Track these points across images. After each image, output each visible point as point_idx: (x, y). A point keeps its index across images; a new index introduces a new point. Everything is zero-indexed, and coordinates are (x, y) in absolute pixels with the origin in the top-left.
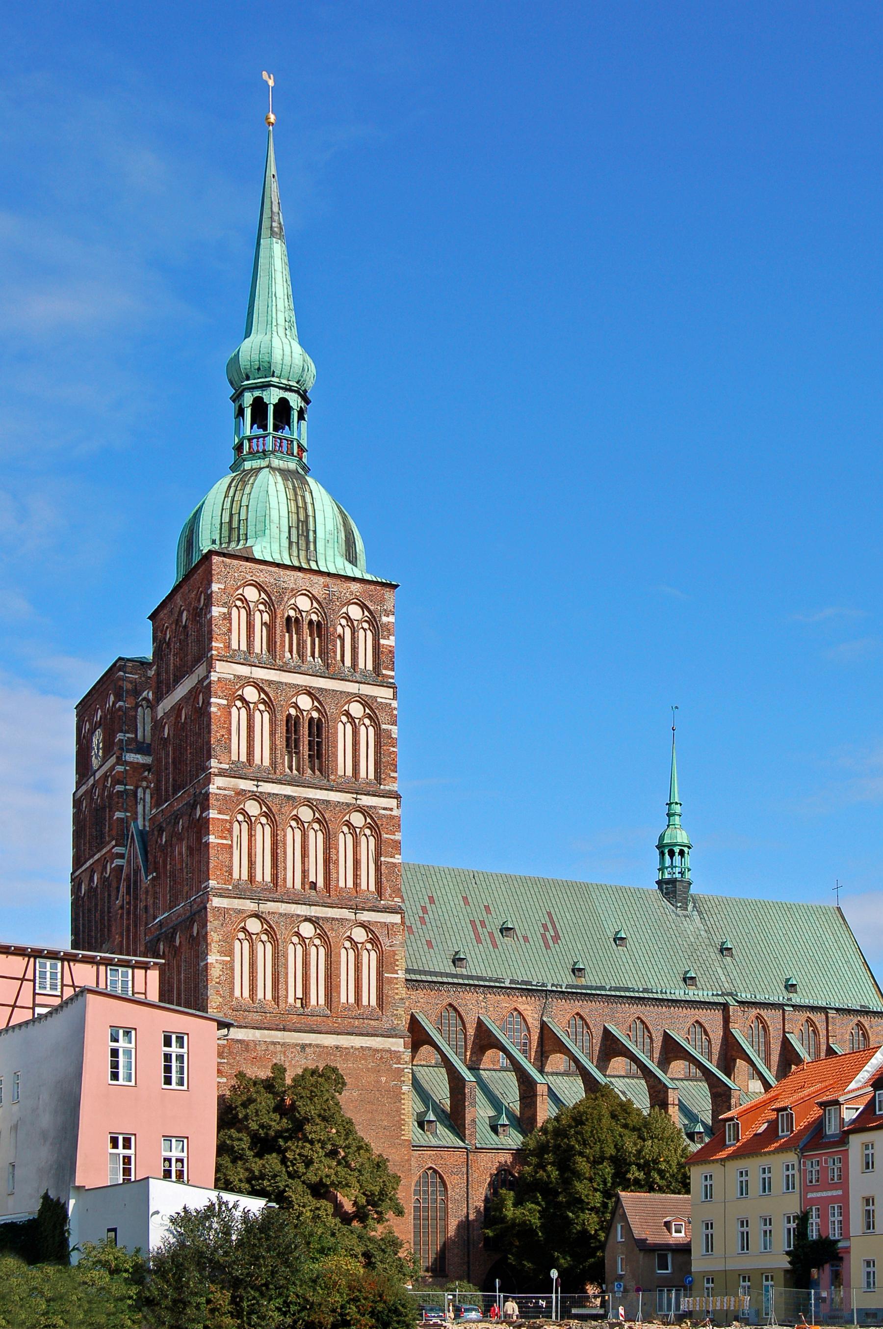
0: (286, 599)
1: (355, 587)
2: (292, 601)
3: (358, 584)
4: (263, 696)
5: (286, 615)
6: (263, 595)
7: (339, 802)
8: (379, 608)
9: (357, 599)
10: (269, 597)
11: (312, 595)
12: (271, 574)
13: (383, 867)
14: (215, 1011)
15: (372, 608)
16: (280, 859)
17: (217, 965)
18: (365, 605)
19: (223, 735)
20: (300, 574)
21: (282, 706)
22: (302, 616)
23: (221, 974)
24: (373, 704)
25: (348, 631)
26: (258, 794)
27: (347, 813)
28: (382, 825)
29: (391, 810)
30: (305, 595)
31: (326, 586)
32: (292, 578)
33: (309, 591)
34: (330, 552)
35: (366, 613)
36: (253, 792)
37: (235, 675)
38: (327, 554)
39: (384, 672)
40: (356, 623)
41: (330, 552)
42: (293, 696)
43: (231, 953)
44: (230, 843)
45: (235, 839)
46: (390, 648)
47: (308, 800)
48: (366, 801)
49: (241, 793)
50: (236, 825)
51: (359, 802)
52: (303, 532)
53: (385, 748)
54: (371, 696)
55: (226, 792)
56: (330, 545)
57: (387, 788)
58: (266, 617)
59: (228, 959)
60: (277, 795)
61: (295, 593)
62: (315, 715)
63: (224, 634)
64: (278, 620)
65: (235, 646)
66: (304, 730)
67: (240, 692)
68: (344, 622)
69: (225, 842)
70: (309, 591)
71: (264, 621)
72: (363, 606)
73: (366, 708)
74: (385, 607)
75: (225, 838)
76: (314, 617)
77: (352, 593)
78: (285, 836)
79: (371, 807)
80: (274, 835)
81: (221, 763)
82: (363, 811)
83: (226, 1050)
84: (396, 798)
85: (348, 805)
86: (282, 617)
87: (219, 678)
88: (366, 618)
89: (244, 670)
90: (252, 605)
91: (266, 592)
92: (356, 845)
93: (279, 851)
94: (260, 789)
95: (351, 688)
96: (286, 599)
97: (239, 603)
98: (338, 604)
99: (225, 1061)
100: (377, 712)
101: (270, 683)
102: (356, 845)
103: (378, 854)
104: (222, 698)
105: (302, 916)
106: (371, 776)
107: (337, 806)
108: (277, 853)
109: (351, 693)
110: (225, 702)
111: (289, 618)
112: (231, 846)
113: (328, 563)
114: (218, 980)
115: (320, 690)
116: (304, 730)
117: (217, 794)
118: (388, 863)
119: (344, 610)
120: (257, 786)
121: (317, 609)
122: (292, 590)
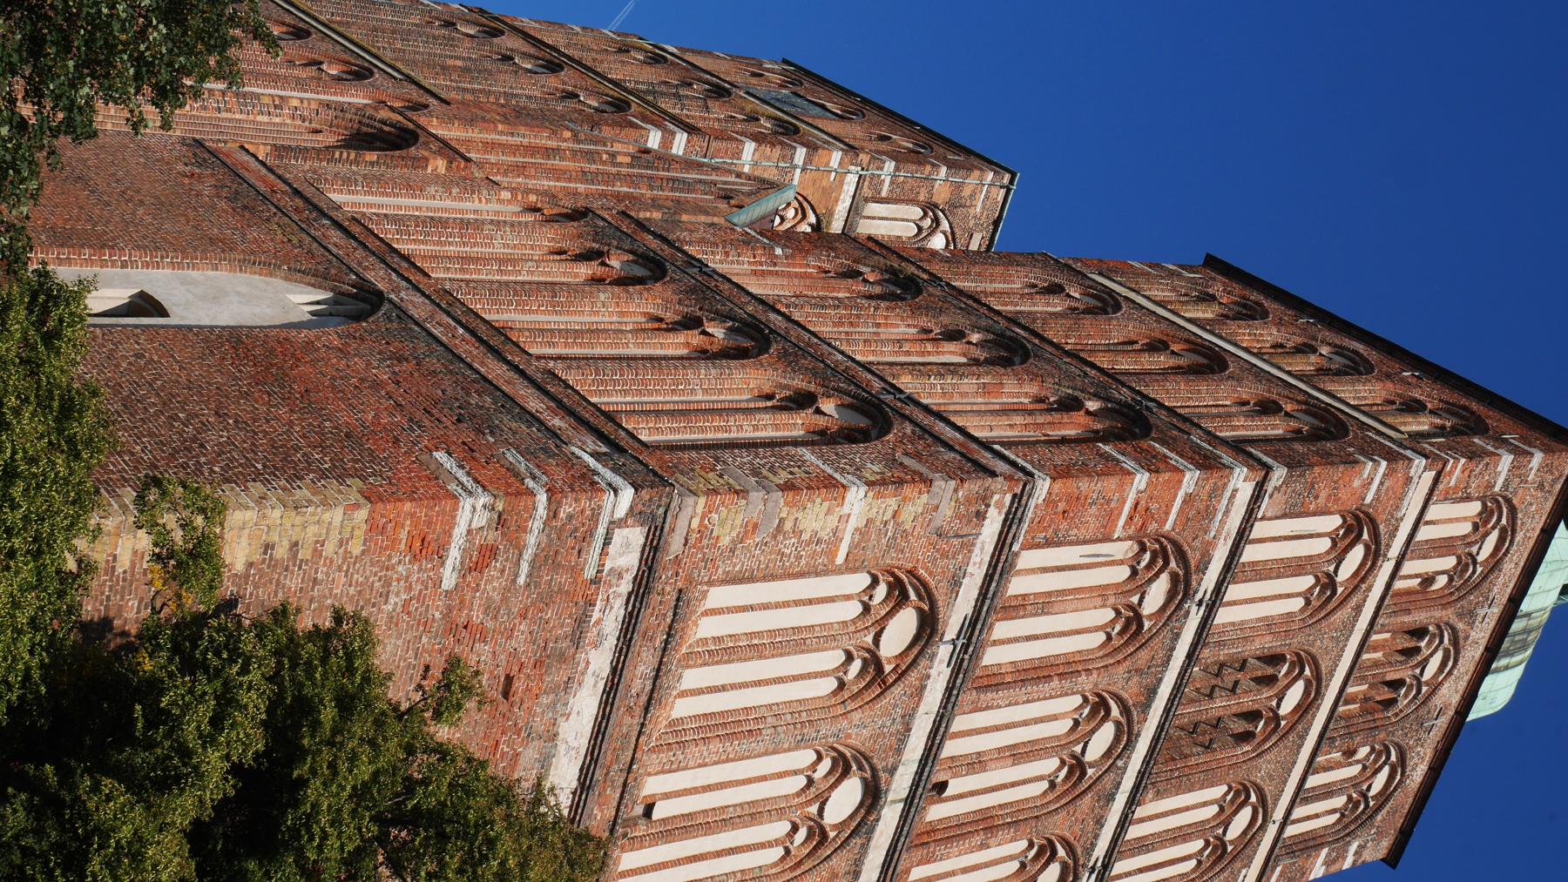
11: (1441, 683)
14: (695, 523)
15: (1379, 818)
17: (832, 521)
18: (1387, 800)
19: (1316, 497)
23: (805, 537)
33: (1450, 673)
36: (1196, 592)
37: (1402, 519)
43: (850, 567)
59: (840, 559)
70: (1450, 673)
72: (1385, 795)
83: (563, 578)
87: (1412, 478)
91: (1485, 577)
99: (521, 580)
105: (889, 784)
109: (1276, 806)
110: (1368, 500)
112: (1107, 539)
114: (788, 526)
117: (1225, 485)
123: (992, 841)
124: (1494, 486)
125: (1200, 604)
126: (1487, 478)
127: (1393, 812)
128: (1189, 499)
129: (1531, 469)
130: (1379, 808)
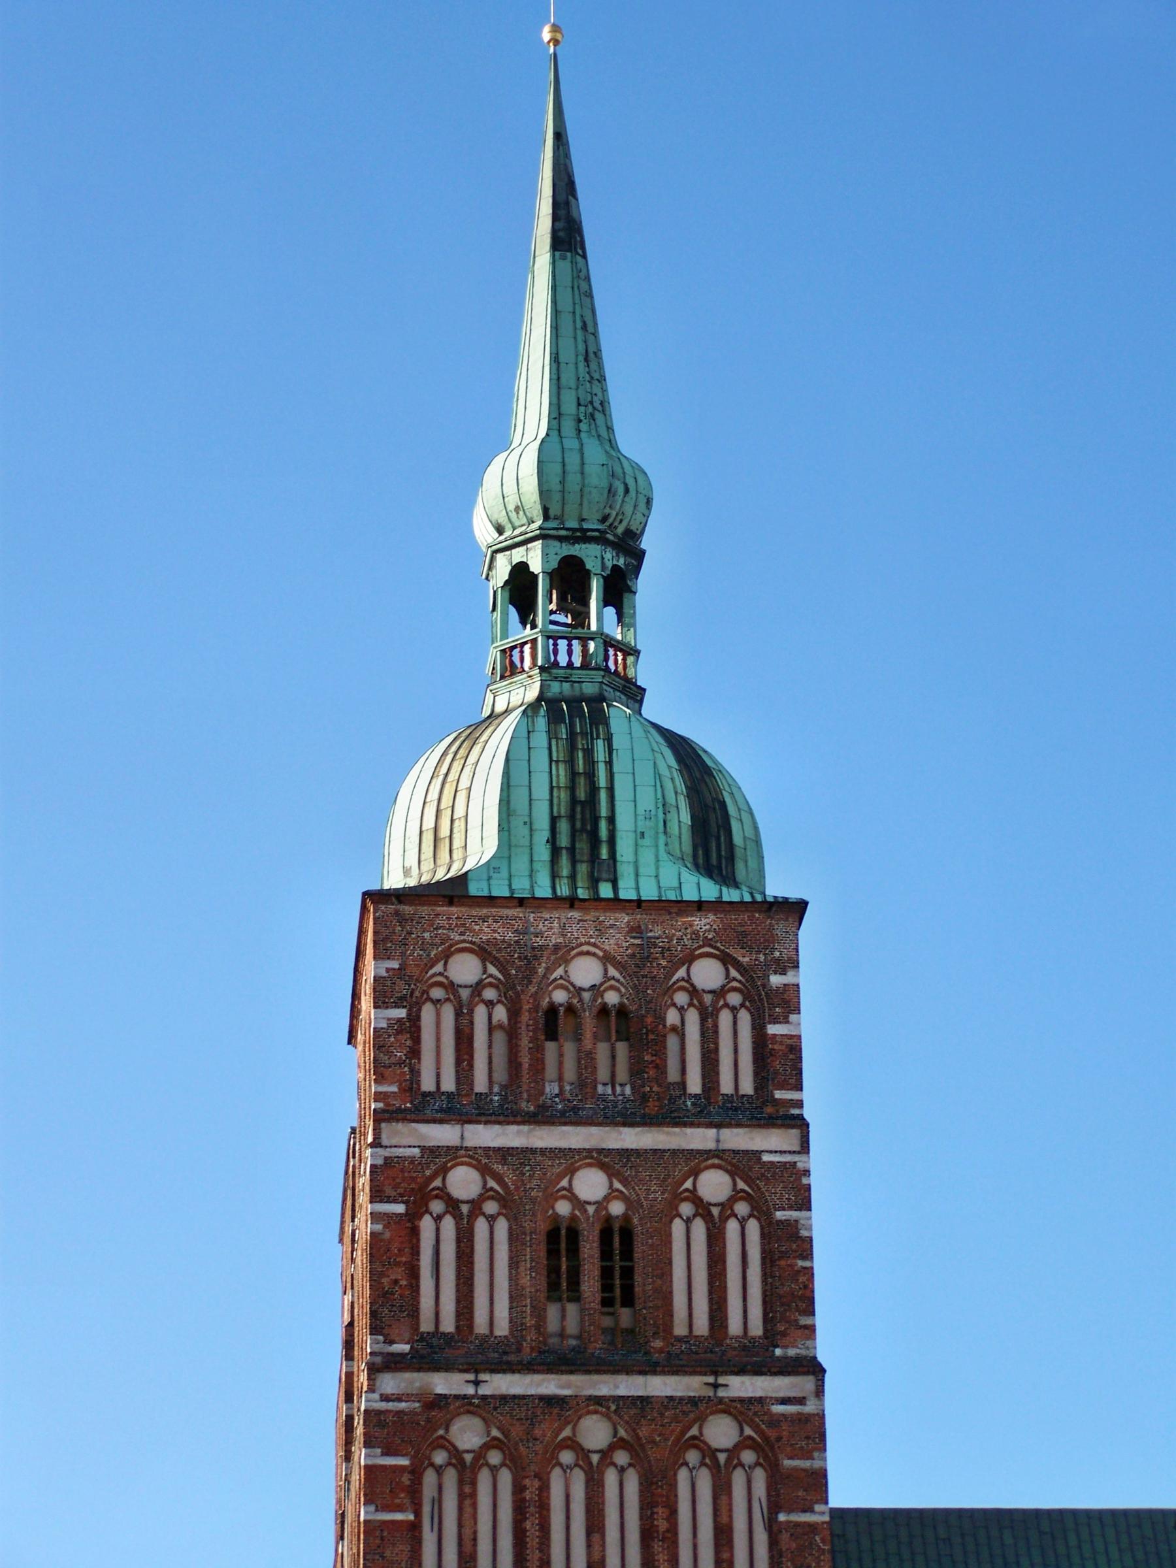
0: (541, 971)
1: (702, 923)
2: (560, 972)
3: (711, 917)
4: (492, 1183)
5: (545, 1003)
6: (492, 970)
7: (671, 1398)
8: (762, 958)
9: (711, 946)
10: (502, 969)
12: (506, 921)
13: (785, 1537)
16: (532, 1540)
18: (729, 955)
19: (396, 1282)
20: (575, 914)
21: (533, 1200)
22: (581, 1000)
24: (750, 1169)
25: (693, 1019)
26: (476, 1401)
27: (695, 1421)
28: (779, 1439)
29: (801, 1401)
30: (588, 953)
31: (635, 930)
32: (555, 924)
34: (647, 857)
35: (734, 973)
36: (465, 1397)
37: (423, 1149)
38: (642, 860)
39: (778, 1095)
40: (708, 999)
41: (647, 857)
42: (560, 1177)
44: (411, 1517)
45: (426, 1509)
46: (789, 1042)
47: (599, 1401)
48: (740, 1386)
49: (437, 1403)
50: (430, 1477)
51: (721, 1393)
52: (583, 820)
53: (783, 1263)
54: (746, 1152)
55: (403, 1405)
56: (647, 841)
57: (792, 1352)
58: (500, 1014)
60: (523, 1397)
61: (564, 954)
62: (617, 1208)
63: (401, 1063)
64: (525, 1017)
65: (427, 1084)
66: (590, 1249)
67: (437, 1183)
68: (681, 998)
69: (399, 1516)
70: (594, 945)
71: (495, 1021)
72: (726, 960)
73: (738, 1180)
74: (777, 954)
75: (400, 1509)
76: (612, 998)
77: (696, 933)
78: (544, 1488)
79: (751, 1400)
80: (518, 1489)
81: (392, 1342)
82: (742, 1410)
84: (814, 1373)
85: (693, 1401)
86: (536, 1008)
87: (386, 1158)
88: (735, 984)
89: (444, 1134)
90: (465, 994)
91: (496, 962)
92: (722, 1490)
93: (528, 1525)
94: (484, 1390)
95: (700, 1138)
96: (541, 971)
97: (437, 993)
98: (664, 963)
100: (762, 1184)
101: (504, 1153)
102: (722, 1490)
103: (774, 1506)
104: (395, 1201)
106: (756, 1328)
107: (666, 1408)
108: (524, 1531)
110: (400, 1208)
111: (553, 1010)
112: (415, 1527)
113: (642, 880)
115: (626, 1153)
116: (590, 1249)
118: (797, 1525)
119: (681, 973)
120: (477, 1383)
121: (618, 981)
122: (557, 947)
123: (662, 1525)
124: (399, 1020)
125: (477, 1383)
126: (392, 1039)
127: (743, 939)
128: (386, 1453)
129: (388, 970)
130: (738, 966)
